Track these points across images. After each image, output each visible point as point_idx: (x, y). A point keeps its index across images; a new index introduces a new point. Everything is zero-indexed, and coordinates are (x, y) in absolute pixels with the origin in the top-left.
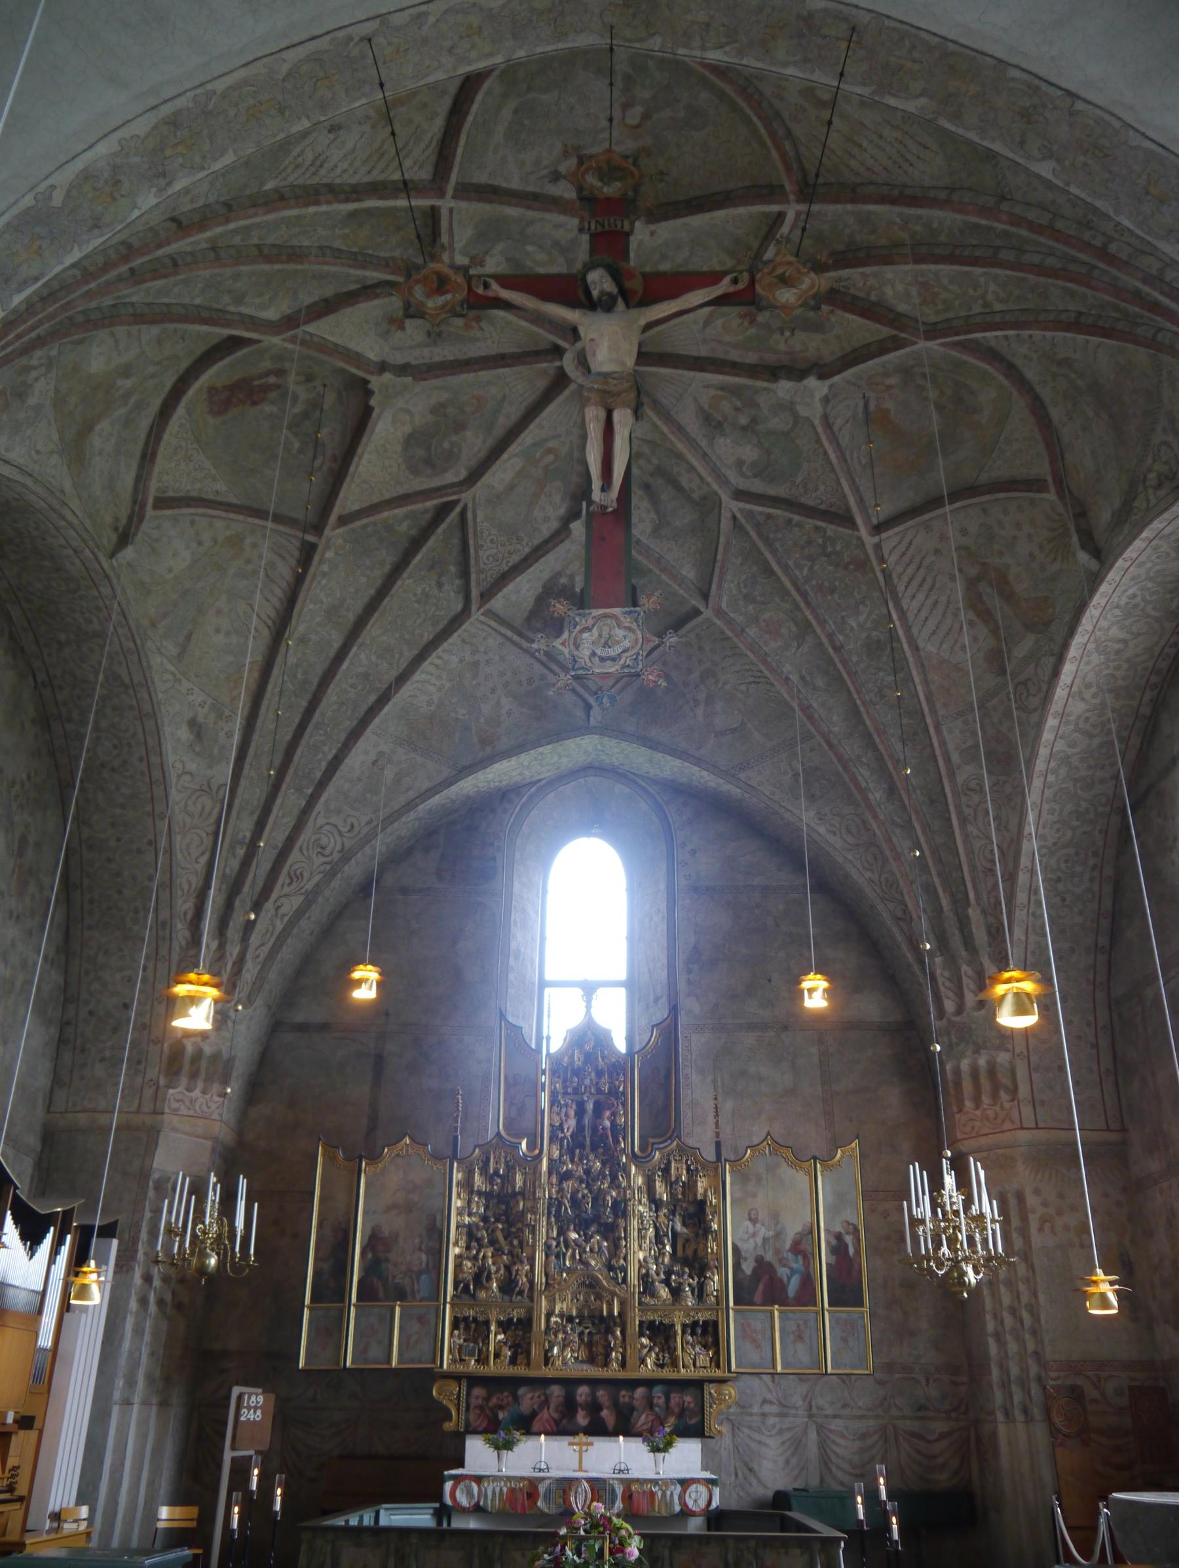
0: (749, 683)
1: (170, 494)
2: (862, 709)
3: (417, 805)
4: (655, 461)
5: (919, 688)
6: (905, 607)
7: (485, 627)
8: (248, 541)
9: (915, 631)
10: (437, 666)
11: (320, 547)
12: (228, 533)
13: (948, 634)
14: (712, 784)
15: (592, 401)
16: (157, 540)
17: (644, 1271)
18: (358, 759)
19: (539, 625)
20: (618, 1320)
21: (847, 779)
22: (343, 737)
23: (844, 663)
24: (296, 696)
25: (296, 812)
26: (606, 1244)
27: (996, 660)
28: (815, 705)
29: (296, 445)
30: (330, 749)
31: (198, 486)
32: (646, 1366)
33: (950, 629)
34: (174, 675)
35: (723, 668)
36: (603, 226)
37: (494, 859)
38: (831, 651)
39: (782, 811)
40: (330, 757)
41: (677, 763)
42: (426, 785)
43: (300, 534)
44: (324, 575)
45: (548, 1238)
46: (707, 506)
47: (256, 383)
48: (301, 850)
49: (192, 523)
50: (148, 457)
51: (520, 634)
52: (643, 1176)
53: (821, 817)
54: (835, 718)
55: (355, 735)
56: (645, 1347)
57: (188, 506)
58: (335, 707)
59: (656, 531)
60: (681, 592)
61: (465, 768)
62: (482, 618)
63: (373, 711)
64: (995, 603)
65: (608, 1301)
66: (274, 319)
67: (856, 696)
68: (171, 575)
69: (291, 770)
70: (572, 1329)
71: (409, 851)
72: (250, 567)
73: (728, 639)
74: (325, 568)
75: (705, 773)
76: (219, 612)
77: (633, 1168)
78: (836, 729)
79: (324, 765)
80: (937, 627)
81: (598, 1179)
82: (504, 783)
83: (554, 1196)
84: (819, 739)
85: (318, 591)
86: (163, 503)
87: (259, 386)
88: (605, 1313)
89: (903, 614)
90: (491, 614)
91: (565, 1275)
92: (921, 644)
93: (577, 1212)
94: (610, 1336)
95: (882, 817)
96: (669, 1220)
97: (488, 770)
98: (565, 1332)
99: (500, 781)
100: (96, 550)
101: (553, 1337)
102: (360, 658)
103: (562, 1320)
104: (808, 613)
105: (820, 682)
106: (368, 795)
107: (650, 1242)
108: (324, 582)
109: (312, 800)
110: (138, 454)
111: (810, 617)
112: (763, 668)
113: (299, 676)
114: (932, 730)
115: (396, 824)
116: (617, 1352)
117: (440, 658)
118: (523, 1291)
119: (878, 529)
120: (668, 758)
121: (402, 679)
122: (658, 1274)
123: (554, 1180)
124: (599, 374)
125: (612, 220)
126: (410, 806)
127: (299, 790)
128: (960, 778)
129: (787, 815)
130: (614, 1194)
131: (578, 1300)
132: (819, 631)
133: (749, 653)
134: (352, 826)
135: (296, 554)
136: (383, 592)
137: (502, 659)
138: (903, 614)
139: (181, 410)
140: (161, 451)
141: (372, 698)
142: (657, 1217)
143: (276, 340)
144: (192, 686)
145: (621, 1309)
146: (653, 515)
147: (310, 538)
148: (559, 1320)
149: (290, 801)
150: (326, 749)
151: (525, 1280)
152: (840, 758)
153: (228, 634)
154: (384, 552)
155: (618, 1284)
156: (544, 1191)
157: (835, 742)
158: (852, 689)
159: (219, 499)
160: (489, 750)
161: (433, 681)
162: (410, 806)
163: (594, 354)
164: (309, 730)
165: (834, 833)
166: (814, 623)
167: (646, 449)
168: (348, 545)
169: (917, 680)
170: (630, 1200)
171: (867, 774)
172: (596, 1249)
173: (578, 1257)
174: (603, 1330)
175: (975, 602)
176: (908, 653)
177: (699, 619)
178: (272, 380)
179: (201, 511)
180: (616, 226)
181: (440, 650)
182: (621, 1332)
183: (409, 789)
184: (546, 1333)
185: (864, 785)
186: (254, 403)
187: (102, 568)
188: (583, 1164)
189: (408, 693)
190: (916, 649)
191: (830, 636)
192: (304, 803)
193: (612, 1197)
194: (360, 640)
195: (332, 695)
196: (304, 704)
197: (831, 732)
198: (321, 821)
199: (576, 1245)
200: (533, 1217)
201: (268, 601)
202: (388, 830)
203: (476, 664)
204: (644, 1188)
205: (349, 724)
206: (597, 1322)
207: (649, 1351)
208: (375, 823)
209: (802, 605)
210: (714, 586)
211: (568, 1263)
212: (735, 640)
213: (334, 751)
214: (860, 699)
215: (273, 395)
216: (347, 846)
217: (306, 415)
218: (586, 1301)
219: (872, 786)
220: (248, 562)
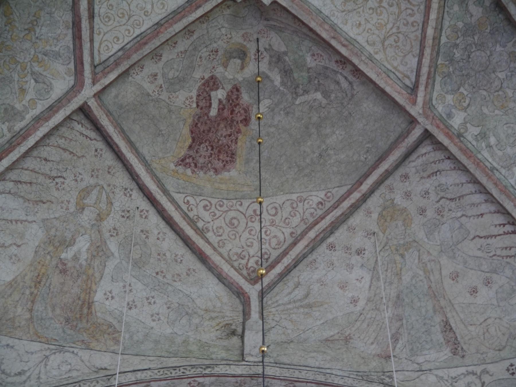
8: (399, 200)
11: (429, 128)
12: (375, 216)
29: (319, 96)
31: (296, 221)
34: (473, 373)
44: (483, 136)
47: (213, 112)
66: (72, 83)
68: (362, 303)
72: (430, 213)
74: (473, 131)
76: (455, 277)
85: (500, 153)
87: (221, 109)
100: (207, 371)
108: (493, 140)
110: (198, 266)
144: (507, 363)
147: (417, 133)
153: (488, 283)
154: (499, 48)
159: (328, 205)
168: (462, 90)
178: (219, 94)
186: (246, 121)
187: (234, 376)
201: (482, 215)
215: (246, 98)
217: (286, 73)
220: (422, 211)
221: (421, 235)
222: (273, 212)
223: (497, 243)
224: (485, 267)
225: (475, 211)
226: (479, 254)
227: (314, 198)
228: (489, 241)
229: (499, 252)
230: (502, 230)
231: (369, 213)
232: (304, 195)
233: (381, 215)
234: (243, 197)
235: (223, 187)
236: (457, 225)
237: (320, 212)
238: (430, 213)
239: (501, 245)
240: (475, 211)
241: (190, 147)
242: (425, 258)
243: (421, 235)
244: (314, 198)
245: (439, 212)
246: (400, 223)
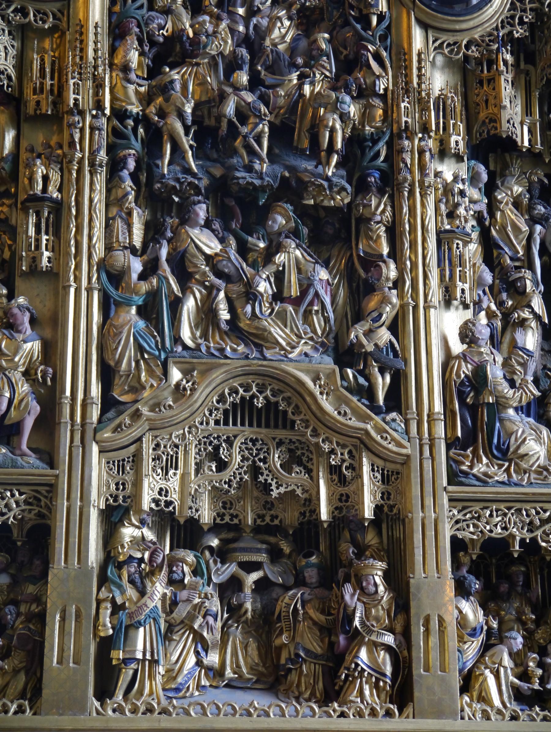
17: (466, 369)
20: (371, 538)
26: (323, 274)
32: (484, 698)
45: (109, 248)
52: (450, 64)
56: (473, 633)
65: (334, 470)
70: (196, 572)
77: (418, 34)
81: (294, 66)
83: (135, 109)
88: (324, 515)
91: (176, 375)
93: (218, 172)
94: (348, 589)
96: (533, 221)
98: (171, 582)
101: (131, 592)
103: (161, 537)
107: (479, 282)
116: (374, 646)
118: (17, 427)
122: (512, 384)
123: (134, 57)
130: (353, 110)
131: (222, 466)
142: (492, 206)
145: (385, 495)
148: (150, 535)
151: (23, 388)
155: (377, 410)
156: (99, 86)
170: (410, 135)
172: (295, 291)
173: (225, 315)
174: (311, 575)
182: (386, 576)
184: (103, 580)
188: (232, 15)
193: (344, 117)
199: (219, 274)
200: (55, 177)
204: (457, 102)
206: (287, 549)
207: (486, 647)
211: (186, 334)
218: (255, 471)
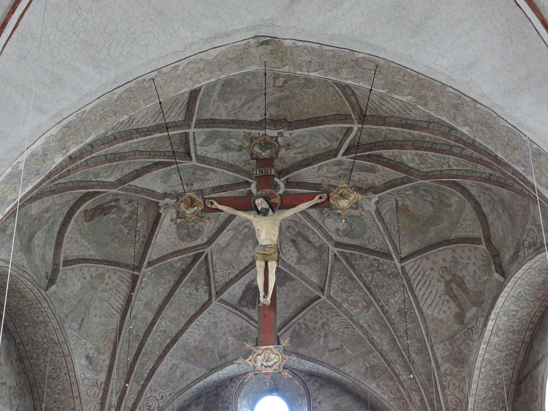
0: (344, 328)
1: (70, 258)
2: (397, 340)
3: (191, 387)
4: (297, 230)
5: (423, 330)
6: (417, 294)
7: (219, 306)
9: (421, 304)
10: (197, 325)
12: (97, 273)
13: (437, 306)
14: (329, 373)
15: (259, 258)
16: (65, 279)
18: (163, 368)
19: (244, 304)
21: (390, 370)
22: (156, 359)
23: (388, 319)
24: (133, 342)
25: (137, 392)
27: (460, 317)
28: (375, 338)
30: (150, 364)
31: (82, 253)
33: (438, 304)
35: (332, 322)
36: (262, 173)
37: (228, 408)
38: (382, 314)
39: (360, 384)
40: (151, 367)
41: (312, 364)
42: (196, 377)
43: (132, 272)
46: (321, 249)
48: (140, 408)
49: (81, 270)
50: (59, 244)
51: (236, 309)
53: (378, 387)
54: (384, 343)
55: (161, 357)
57: (78, 263)
58: (151, 346)
59: (299, 261)
60: (311, 289)
61: (213, 369)
62: (218, 303)
63: (169, 347)
64: (457, 291)
67: (394, 334)
69: (133, 374)
71: (189, 406)
72: (108, 287)
73: (334, 308)
75: (324, 368)
78: (385, 348)
79: (148, 371)
80: (432, 303)
82: (231, 374)
84: (377, 353)
86: (67, 263)
89: (415, 297)
90: (223, 301)
92: (424, 310)
95: (406, 387)
97: (224, 370)
99: (230, 374)
102: (162, 324)
104: (371, 297)
105: (377, 327)
106: (169, 383)
109: (144, 386)
111: (372, 299)
112: (350, 321)
113: (134, 333)
114: (429, 349)
115: (182, 395)
117: (199, 321)
119: (402, 260)
120: (307, 361)
121: (181, 332)
124: (262, 246)
125: (266, 170)
126: (188, 387)
127: (138, 382)
128: (442, 369)
129: (363, 386)
132: (376, 305)
133: (344, 315)
134: (162, 397)
135: (129, 280)
136: (170, 294)
137: (228, 320)
138: (415, 297)
139: (72, 222)
140: (65, 240)
141: (168, 341)
143: (115, 191)
146: (297, 254)
149: (133, 387)
150: (148, 364)
152: (386, 361)
157: (385, 354)
158: (392, 331)
160: (224, 360)
161: (196, 331)
162: (188, 387)
163: (259, 236)
164: (140, 357)
165: (385, 394)
166: (374, 302)
167: (292, 224)
169: (422, 327)
171: (399, 368)
175: (449, 291)
176: (418, 315)
177: (320, 300)
179: (84, 264)
180: (268, 173)
181: (199, 318)
183: (187, 380)
185: (398, 372)
189: (185, 338)
190: (421, 313)
191: (382, 307)
192: (140, 388)
194: (161, 316)
195: (149, 340)
196: (137, 345)
197: (382, 349)
198: (148, 395)
201: (118, 301)
202: (179, 398)
203: (216, 323)
205: (158, 353)
208: (173, 395)
209: (368, 294)
210: (326, 286)
212: (337, 309)
213: (152, 365)
214: (396, 335)
216: (161, 406)
219: (401, 373)
220: (107, 284)
221: (100, 289)
222: (81, 245)
223: (112, 310)
224: (103, 313)
225: (118, 299)
226: (106, 308)
227: (92, 252)
228: (111, 308)
229: (110, 313)
230: (117, 309)
231: (97, 270)
232: (91, 249)
233: (98, 274)
234: (80, 234)
235: (81, 226)
236: (110, 296)
237: (88, 257)
238: (108, 287)
239: (112, 312)
240: (118, 299)
241: (92, 209)
242: (94, 296)
243: (100, 289)
244: (92, 252)
245: (110, 289)
246: (100, 281)
